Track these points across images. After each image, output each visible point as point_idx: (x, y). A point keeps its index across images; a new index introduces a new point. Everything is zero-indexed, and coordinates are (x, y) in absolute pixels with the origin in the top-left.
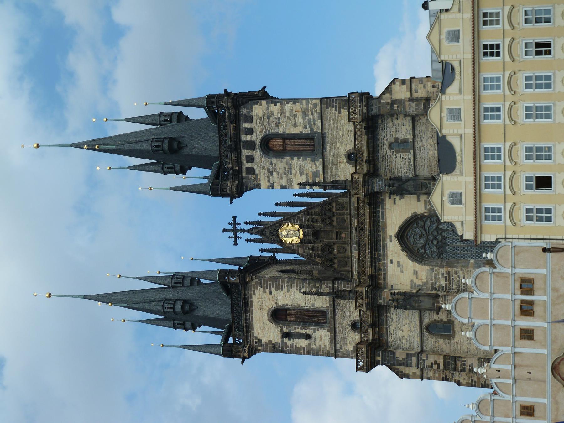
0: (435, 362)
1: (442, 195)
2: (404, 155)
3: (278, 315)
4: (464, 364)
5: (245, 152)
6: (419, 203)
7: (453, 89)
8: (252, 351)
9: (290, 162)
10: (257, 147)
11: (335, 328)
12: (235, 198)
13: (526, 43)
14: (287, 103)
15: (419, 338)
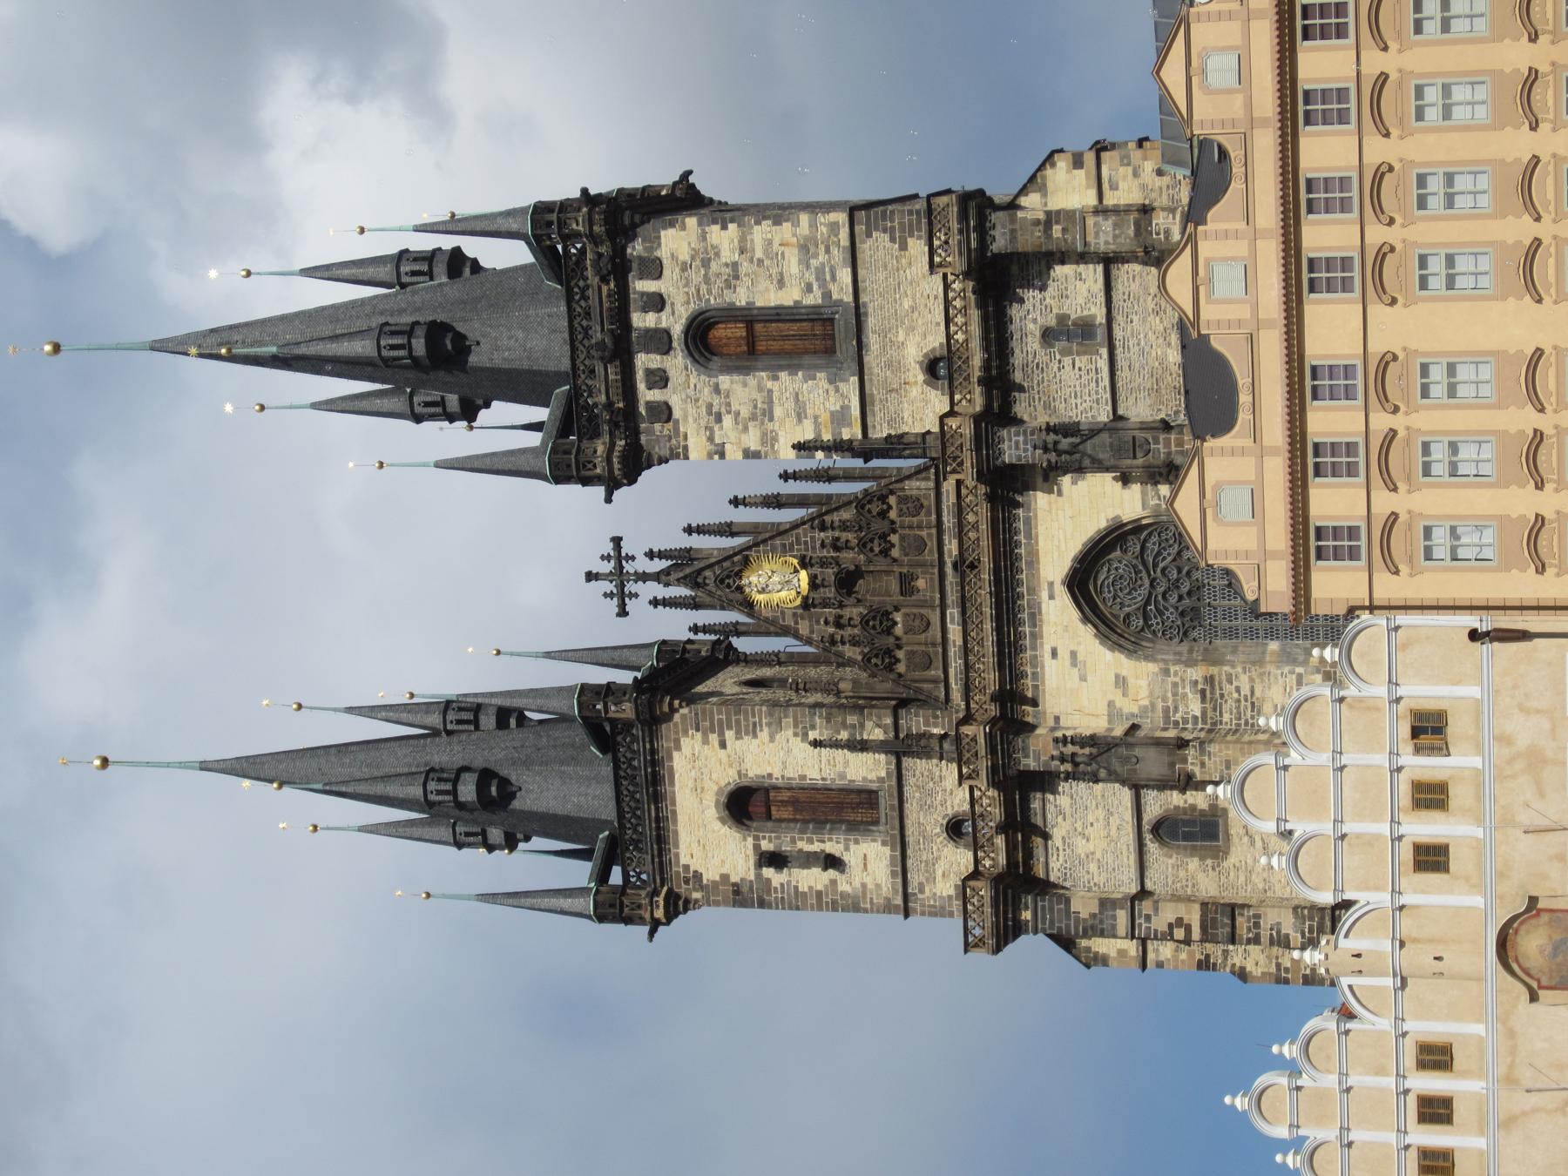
0: (1179, 922)
2: (1082, 361)
3: (744, 804)
4: (1257, 925)
7: (1221, 217)
8: (676, 905)
9: (769, 384)
10: (675, 344)
12: (618, 485)
14: (758, 223)
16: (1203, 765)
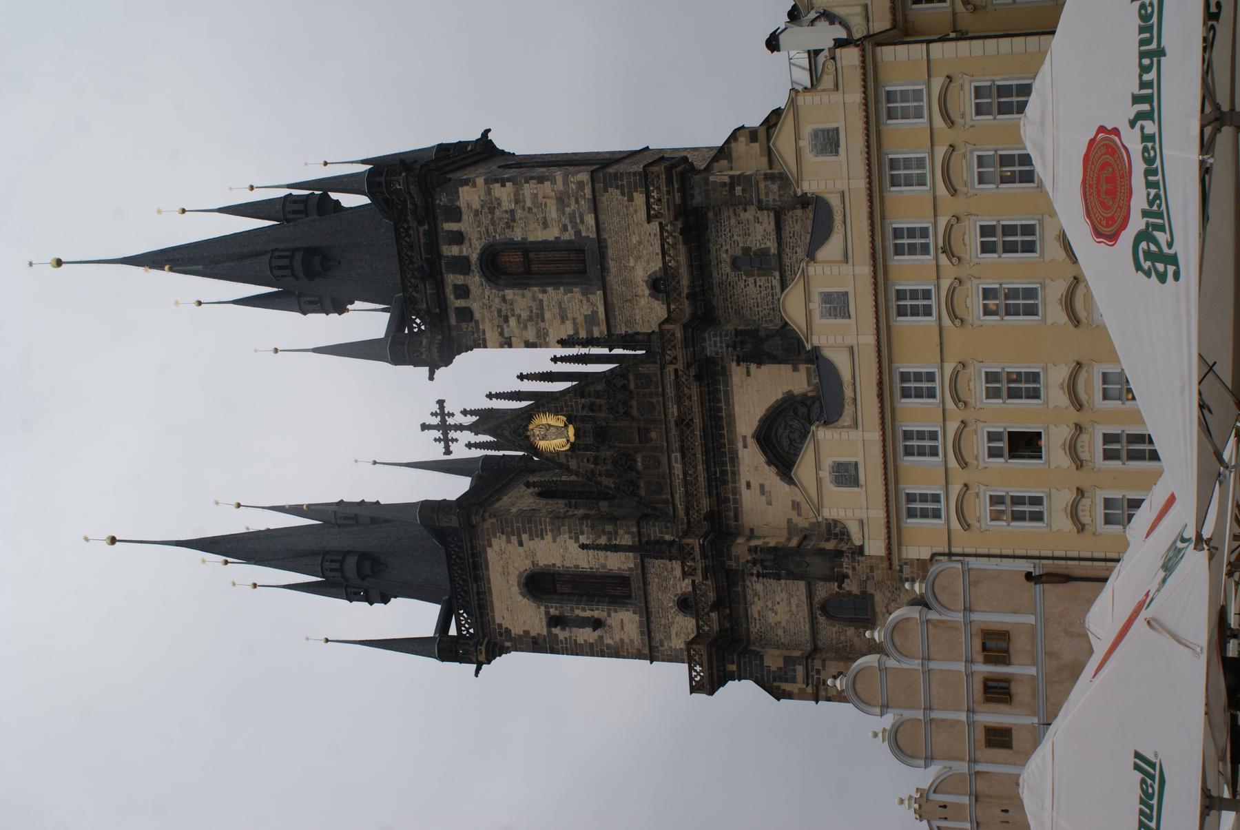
1: (818, 467)
2: (761, 281)
3: (539, 584)
5: (452, 279)
6: (796, 374)
9: (540, 296)
10: (473, 268)
11: (647, 608)
13: (979, 157)
14: (527, 182)
15: (807, 626)
16: (854, 569)
